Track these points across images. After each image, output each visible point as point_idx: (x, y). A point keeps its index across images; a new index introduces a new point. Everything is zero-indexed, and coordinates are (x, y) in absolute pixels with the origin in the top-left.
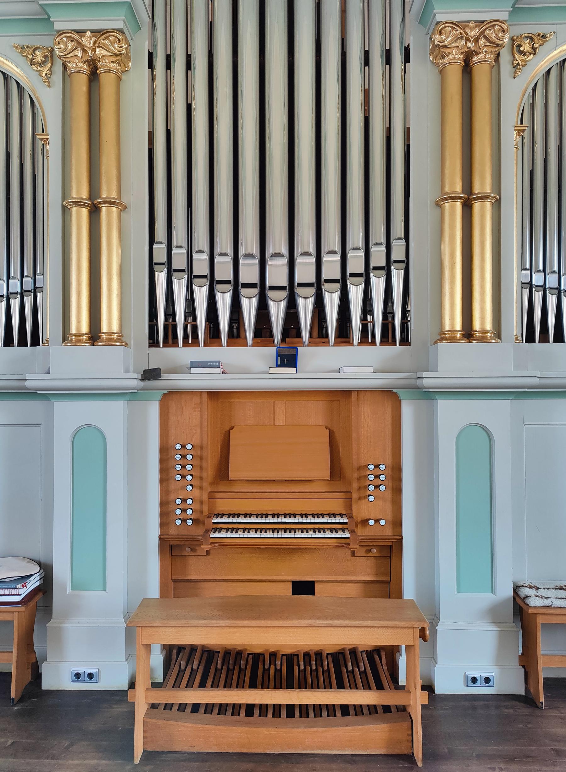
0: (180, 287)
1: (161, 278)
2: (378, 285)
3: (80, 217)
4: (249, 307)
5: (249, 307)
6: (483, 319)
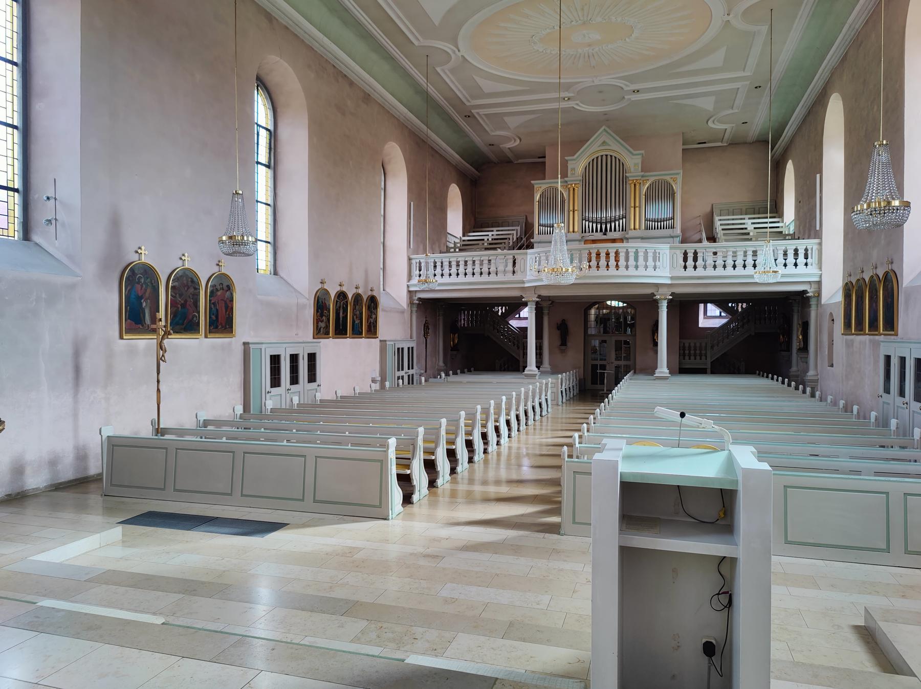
3: (571, 213)
4: (599, 226)
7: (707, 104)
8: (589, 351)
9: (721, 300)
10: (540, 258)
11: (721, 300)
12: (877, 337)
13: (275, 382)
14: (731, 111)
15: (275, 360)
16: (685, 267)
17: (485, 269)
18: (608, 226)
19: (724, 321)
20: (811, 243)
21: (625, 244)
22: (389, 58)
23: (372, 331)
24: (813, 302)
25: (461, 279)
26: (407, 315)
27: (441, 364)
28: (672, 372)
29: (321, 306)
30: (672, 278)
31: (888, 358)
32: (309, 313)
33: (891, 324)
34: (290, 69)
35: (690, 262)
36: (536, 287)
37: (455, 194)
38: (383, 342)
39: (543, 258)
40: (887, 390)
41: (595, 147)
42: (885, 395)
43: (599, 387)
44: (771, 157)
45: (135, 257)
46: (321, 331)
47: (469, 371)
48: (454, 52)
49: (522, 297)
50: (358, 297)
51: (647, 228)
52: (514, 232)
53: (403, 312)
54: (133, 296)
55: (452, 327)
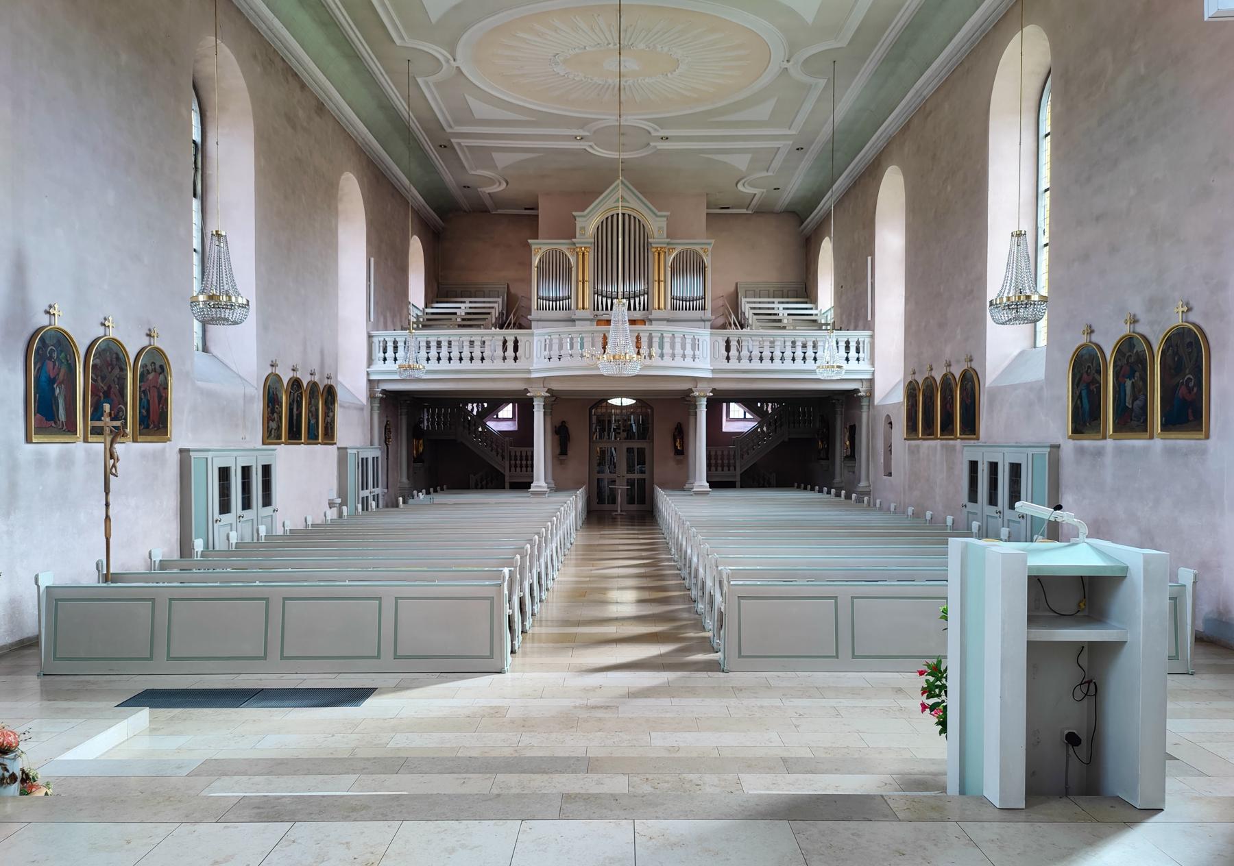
3: (580, 284)
6: (662, 306)
7: (741, 163)
8: (603, 460)
9: (749, 399)
10: (551, 340)
11: (749, 399)
12: (951, 442)
13: (225, 508)
14: (765, 174)
15: (224, 473)
16: (728, 358)
17: (466, 354)
19: (754, 424)
20: (863, 335)
21: (647, 327)
22: (354, 57)
23: (329, 436)
24: (865, 403)
25: (444, 364)
26: (367, 413)
27: (405, 480)
28: (714, 485)
29: (271, 400)
30: (713, 371)
31: (973, 465)
32: (258, 408)
33: (970, 427)
34: (233, 58)
35: (733, 352)
36: (545, 378)
37: (416, 248)
38: (343, 450)
39: (556, 341)
40: (973, 497)
41: (610, 203)
42: (970, 505)
43: (607, 507)
44: (801, 231)
45: (44, 320)
46: (271, 435)
47: (442, 489)
48: (448, 61)
49: (526, 391)
50: (313, 386)
51: (673, 308)
52: (496, 306)
53: (362, 409)
54: (43, 378)
55: (415, 432)
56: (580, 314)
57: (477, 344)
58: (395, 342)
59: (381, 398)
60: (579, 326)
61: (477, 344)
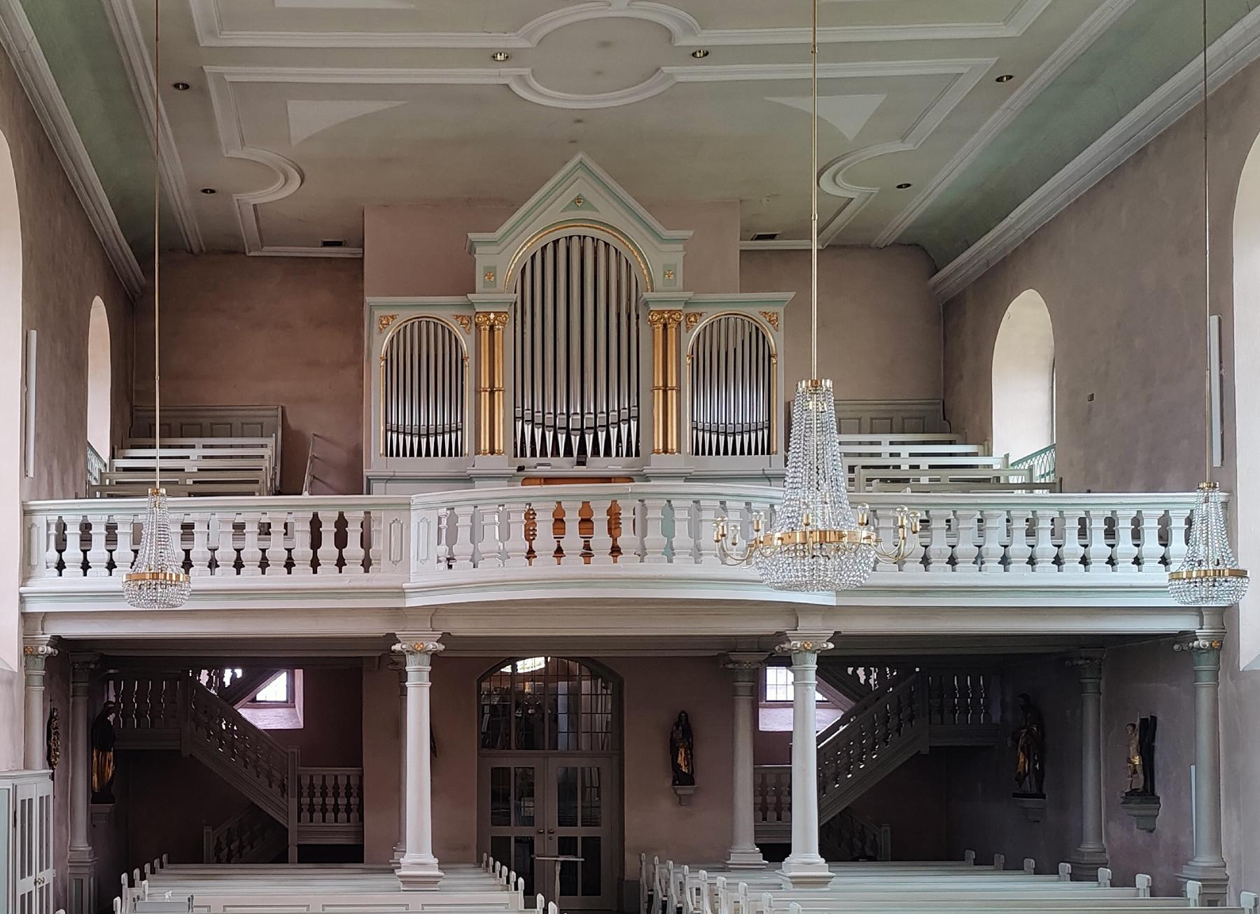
0: (528, 428)
1: (519, 424)
2: (624, 428)
3: (485, 397)
4: (562, 439)
5: (562, 439)
6: (673, 445)
18: (589, 439)
56: (485, 463)
57: (251, 529)
58: (86, 527)
59: (49, 658)
60: (481, 490)
61: (251, 529)
